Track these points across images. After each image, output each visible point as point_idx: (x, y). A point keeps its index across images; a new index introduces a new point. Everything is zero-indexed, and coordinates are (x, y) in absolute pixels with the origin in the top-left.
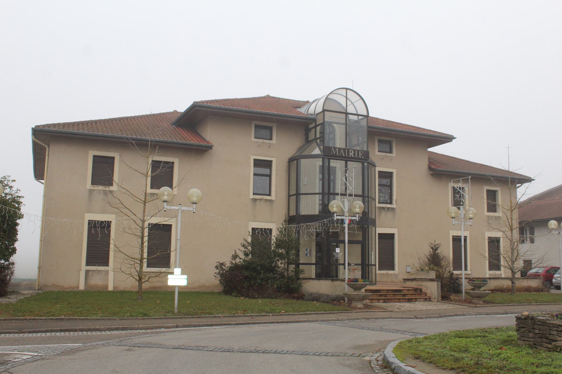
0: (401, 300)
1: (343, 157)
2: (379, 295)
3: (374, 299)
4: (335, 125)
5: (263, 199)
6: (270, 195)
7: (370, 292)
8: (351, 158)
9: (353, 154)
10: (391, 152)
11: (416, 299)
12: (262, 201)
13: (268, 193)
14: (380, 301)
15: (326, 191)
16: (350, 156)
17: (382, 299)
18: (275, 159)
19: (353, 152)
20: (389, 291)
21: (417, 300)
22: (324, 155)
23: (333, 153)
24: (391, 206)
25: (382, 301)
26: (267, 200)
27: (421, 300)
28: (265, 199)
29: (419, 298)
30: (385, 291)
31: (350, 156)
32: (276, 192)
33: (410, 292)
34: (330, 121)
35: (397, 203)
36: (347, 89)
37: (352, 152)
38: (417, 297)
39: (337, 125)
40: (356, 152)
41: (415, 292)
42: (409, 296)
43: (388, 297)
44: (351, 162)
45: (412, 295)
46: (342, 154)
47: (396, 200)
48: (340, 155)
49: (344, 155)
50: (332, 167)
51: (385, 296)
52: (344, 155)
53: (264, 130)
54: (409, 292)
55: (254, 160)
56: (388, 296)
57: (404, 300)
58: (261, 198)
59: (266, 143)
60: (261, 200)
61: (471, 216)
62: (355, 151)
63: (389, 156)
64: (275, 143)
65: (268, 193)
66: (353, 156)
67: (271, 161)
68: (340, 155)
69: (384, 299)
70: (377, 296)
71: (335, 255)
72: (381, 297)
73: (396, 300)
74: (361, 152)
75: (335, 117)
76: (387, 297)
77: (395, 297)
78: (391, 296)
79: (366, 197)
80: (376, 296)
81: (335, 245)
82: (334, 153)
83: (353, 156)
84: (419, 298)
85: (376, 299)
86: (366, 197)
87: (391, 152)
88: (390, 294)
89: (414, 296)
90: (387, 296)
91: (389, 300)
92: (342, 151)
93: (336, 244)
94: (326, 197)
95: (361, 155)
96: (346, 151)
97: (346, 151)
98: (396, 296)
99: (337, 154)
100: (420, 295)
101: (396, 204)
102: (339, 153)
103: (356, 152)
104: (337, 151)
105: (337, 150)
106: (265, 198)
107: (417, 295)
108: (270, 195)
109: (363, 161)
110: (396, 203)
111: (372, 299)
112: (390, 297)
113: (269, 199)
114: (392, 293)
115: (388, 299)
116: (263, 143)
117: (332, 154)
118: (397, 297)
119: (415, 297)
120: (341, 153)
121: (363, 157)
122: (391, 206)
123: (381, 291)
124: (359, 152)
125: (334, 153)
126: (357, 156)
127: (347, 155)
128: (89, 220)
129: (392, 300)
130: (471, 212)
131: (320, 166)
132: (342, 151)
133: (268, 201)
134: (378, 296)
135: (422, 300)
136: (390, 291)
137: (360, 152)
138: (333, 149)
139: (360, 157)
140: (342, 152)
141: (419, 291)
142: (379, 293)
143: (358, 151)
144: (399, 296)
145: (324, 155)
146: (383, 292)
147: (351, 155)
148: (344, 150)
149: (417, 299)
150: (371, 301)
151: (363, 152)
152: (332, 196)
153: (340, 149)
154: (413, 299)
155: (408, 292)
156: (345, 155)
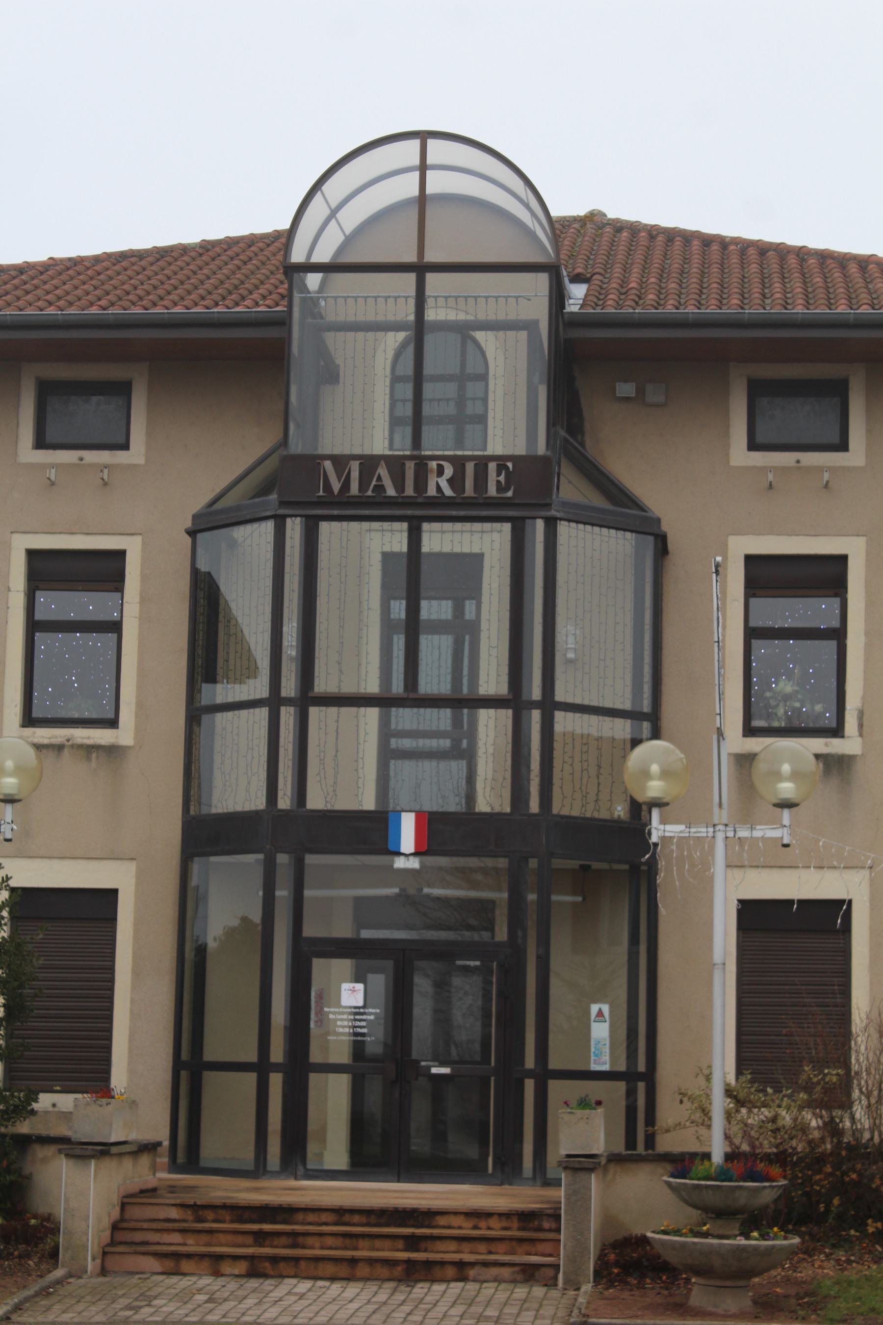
0: (363, 1270)
1: (390, 503)
2: (405, 1238)
3: (189, 1256)
4: (479, 335)
5: (72, 746)
6: (113, 723)
7: (228, 1218)
8: (440, 501)
9: (450, 481)
10: (843, 446)
11: (461, 1265)
12: (66, 751)
13: (36, 713)
14: (227, 1268)
15: (289, 687)
16: (432, 491)
17: (236, 1258)
18: (138, 539)
19: (449, 471)
20: (347, 1218)
21: (472, 1273)
22: (283, 504)
23: (328, 487)
24: (826, 745)
25: (242, 1267)
26: (89, 750)
27: (494, 1271)
28: (81, 746)
29: (486, 1264)
30: (324, 1217)
31: (432, 491)
32: (140, 706)
33: (489, 1228)
34: (462, 317)
35: (865, 729)
36: (424, 136)
37: (440, 471)
38: (468, 1257)
39: (501, 334)
40: (470, 467)
41: (519, 1229)
42: (452, 1246)
43: (312, 1247)
44: (335, 525)
45: (466, 1246)
46: (380, 488)
47: (861, 715)
48: (369, 493)
49: (391, 492)
50: (431, 555)
51: (289, 1241)
52: (391, 492)
53: (95, 399)
54: (483, 1224)
55: (32, 554)
56: (310, 1241)
57: (384, 1271)
58: (54, 741)
59: (91, 465)
60: (59, 748)
61: (787, 789)
62: (459, 463)
63: (820, 470)
64: (141, 461)
65: (757, 723)
66: (448, 492)
67: (120, 555)
68: (369, 493)
69: (250, 1258)
70: (240, 1239)
71: (336, 1020)
72: (261, 1246)
73: (330, 1269)
74: (501, 468)
75: (386, 298)
76: (304, 1247)
77: (356, 1249)
78: (330, 1241)
79: (289, 702)
80: (229, 1238)
81: (476, 967)
82: (336, 486)
83: (448, 492)
84: (486, 1264)
85: (202, 1256)
86: (289, 702)
87: (843, 446)
88: (321, 1234)
89: (482, 1247)
90: (300, 1240)
91: (282, 1265)
92: (382, 471)
93: (478, 963)
94: (288, 716)
95: (498, 482)
96: (410, 467)
97: (410, 467)
98: (361, 1243)
99: (354, 489)
100: (526, 1247)
101: (861, 735)
102: (363, 486)
103: (470, 467)
104: (355, 475)
105: (355, 466)
106: (79, 741)
107: (501, 1247)
108: (113, 723)
109: (409, 512)
110: (861, 726)
111: (177, 1256)
112: (322, 1248)
113: (103, 742)
114: (368, 1225)
115: (275, 1260)
116: (80, 464)
117: (321, 493)
118: (373, 1249)
119: (456, 1257)
120: (374, 483)
121: (510, 494)
122: (826, 745)
123: (300, 1216)
124: (486, 466)
125: (336, 486)
126: (476, 488)
127: (409, 491)
128: (850, 901)
129: (303, 1264)
130: (786, 768)
131: (387, 557)
132: (382, 471)
133: (94, 755)
134: (249, 1240)
135: (506, 1272)
136: (356, 1218)
137: (492, 466)
138: (328, 464)
139: (492, 491)
140: (379, 478)
141: (546, 1225)
142: (285, 1222)
143: (482, 463)
144: (378, 1243)
145: (283, 504)
146: (311, 1217)
147: (439, 489)
148: (396, 464)
149: (472, 1264)
150: (169, 1264)
151: (510, 465)
152: (465, 711)
153: (369, 463)
154: (442, 1263)
155: (475, 1227)
156: (399, 483)
